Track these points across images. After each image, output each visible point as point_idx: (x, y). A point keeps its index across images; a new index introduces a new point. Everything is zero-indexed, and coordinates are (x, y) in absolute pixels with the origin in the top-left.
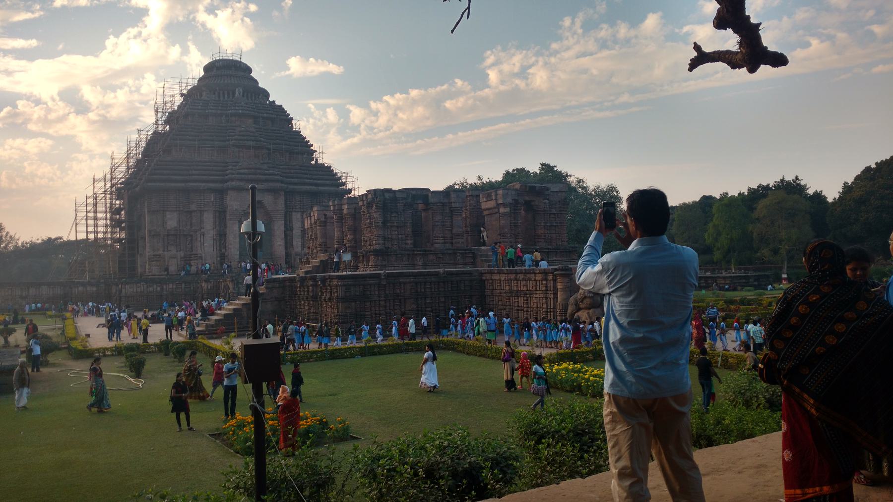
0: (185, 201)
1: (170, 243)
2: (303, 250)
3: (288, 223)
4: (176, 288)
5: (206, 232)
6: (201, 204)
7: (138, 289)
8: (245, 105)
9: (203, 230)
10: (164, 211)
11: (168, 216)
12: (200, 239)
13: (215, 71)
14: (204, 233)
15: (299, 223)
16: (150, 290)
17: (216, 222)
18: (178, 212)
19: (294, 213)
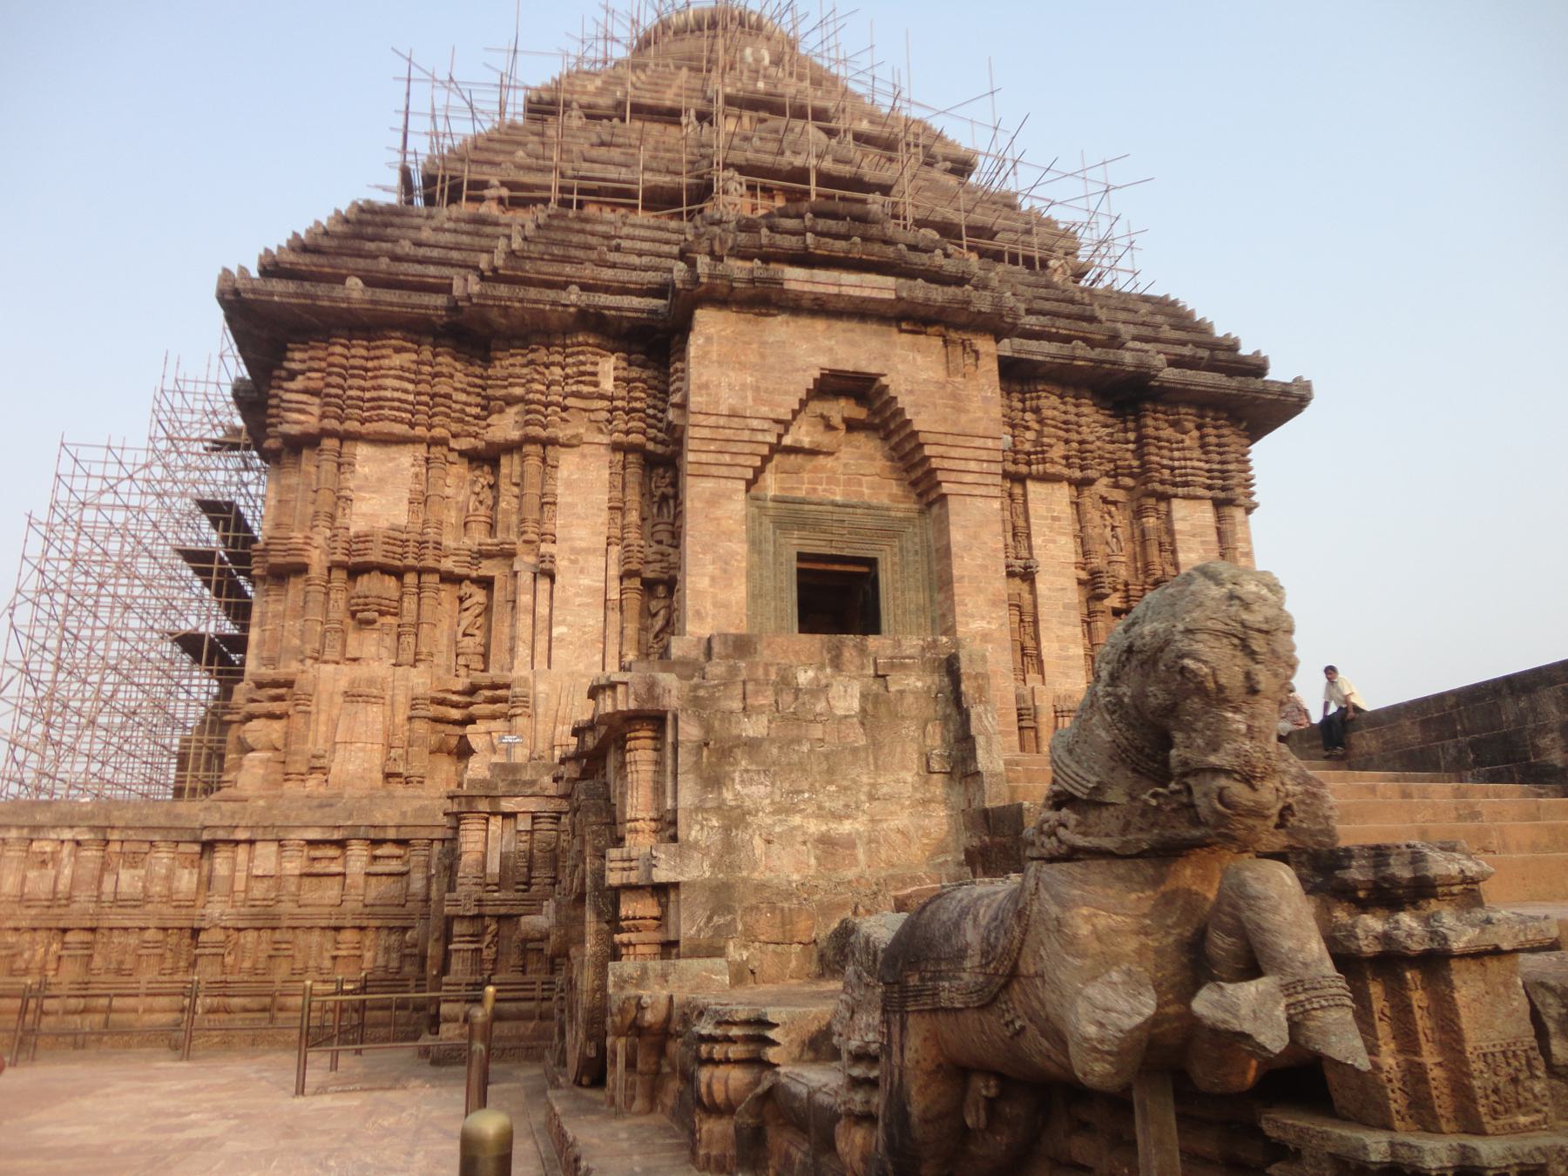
0: (463, 397)
5: (561, 564)
6: (547, 405)
7: (32, 874)
16: (124, 887)
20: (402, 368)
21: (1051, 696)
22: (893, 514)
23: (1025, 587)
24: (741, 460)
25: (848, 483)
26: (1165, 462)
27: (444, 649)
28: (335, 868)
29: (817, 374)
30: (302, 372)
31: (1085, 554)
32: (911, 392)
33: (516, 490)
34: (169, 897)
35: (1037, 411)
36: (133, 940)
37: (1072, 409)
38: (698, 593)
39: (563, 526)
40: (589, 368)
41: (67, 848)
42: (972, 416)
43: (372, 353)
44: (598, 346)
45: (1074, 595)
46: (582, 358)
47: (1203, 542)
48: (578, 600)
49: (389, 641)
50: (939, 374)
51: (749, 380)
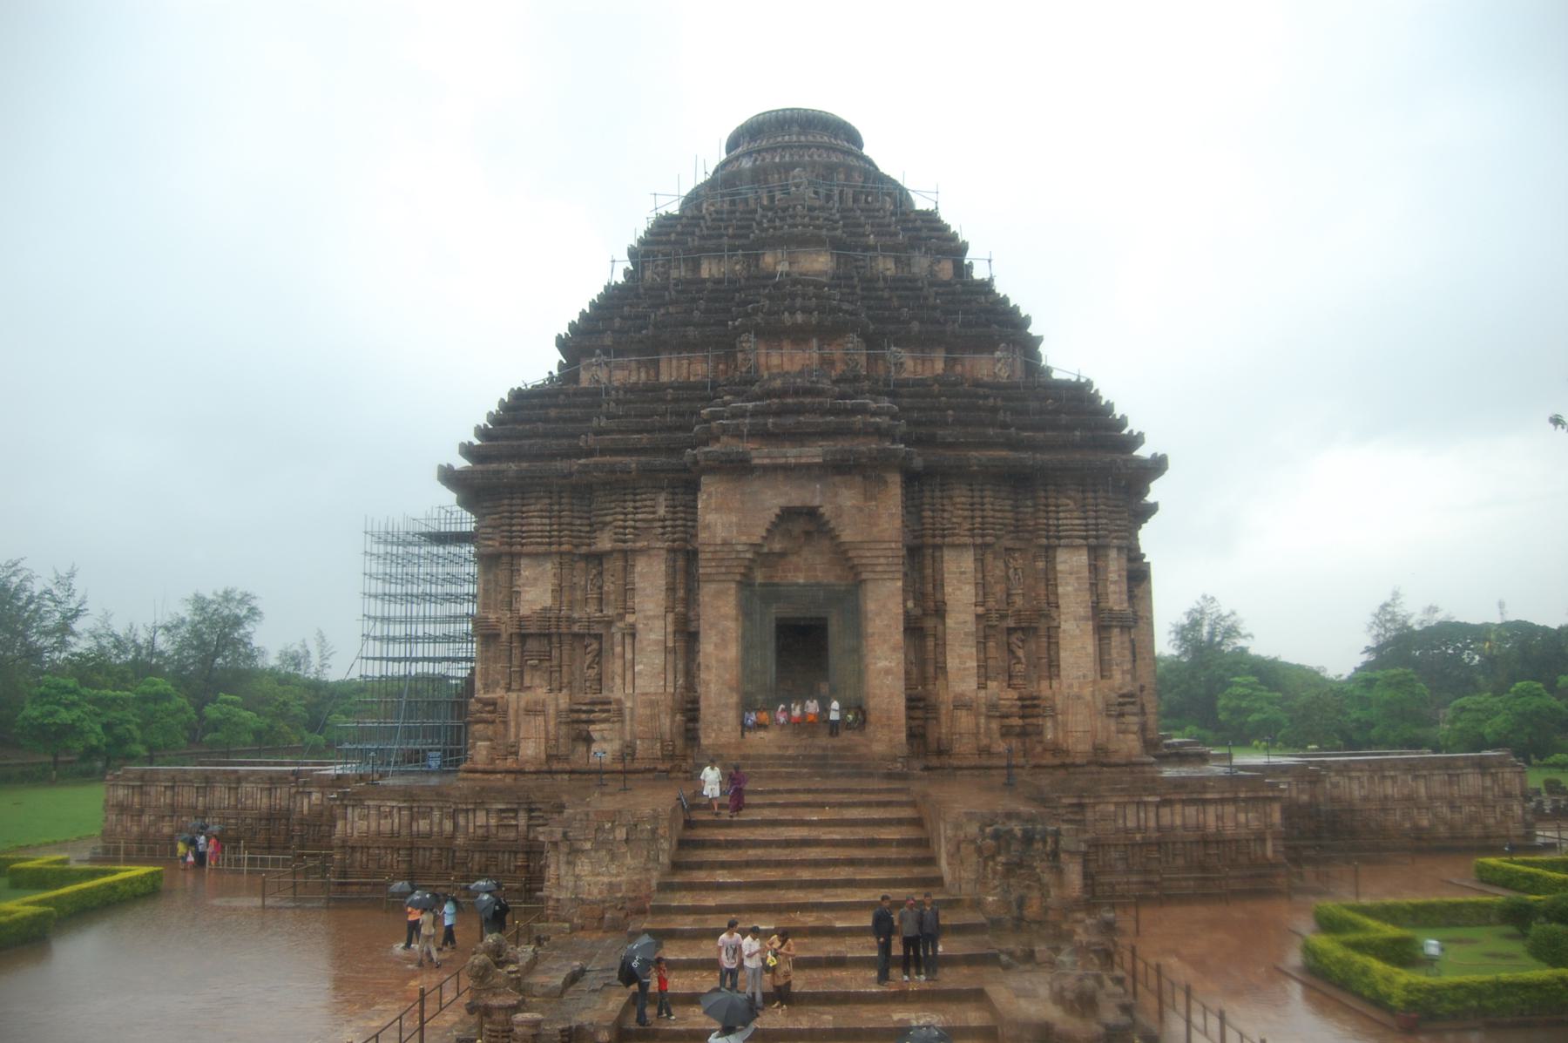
0: (578, 522)
1: (529, 662)
2: (983, 686)
3: (930, 588)
5: (640, 626)
6: (625, 528)
7: (382, 822)
8: (805, 212)
9: (630, 619)
10: (513, 555)
11: (525, 573)
13: (746, 145)
14: (633, 626)
16: (421, 829)
18: (557, 560)
19: (948, 555)
20: (542, 511)
21: (952, 695)
22: (837, 588)
24: (733, 570)
26: (1051, 522)
27: (577, 677)
28: (513, 822)
29: (777, 511)
30: (489, 514)
31: (985, 595)
33: (613, 579)
34: (441, 832)
35: (951, 498)
36: (428, 853)
37: (977, 494)
39: (639, 603)
40: (648, 503)
41: (395, 810)
43: (525, 502)
44: (654, 487)
45: (971, 627)
46: (644, 496)
47: (1078, 578)
48: (649, 649)
49: (546, 676)
51: (734, 519)
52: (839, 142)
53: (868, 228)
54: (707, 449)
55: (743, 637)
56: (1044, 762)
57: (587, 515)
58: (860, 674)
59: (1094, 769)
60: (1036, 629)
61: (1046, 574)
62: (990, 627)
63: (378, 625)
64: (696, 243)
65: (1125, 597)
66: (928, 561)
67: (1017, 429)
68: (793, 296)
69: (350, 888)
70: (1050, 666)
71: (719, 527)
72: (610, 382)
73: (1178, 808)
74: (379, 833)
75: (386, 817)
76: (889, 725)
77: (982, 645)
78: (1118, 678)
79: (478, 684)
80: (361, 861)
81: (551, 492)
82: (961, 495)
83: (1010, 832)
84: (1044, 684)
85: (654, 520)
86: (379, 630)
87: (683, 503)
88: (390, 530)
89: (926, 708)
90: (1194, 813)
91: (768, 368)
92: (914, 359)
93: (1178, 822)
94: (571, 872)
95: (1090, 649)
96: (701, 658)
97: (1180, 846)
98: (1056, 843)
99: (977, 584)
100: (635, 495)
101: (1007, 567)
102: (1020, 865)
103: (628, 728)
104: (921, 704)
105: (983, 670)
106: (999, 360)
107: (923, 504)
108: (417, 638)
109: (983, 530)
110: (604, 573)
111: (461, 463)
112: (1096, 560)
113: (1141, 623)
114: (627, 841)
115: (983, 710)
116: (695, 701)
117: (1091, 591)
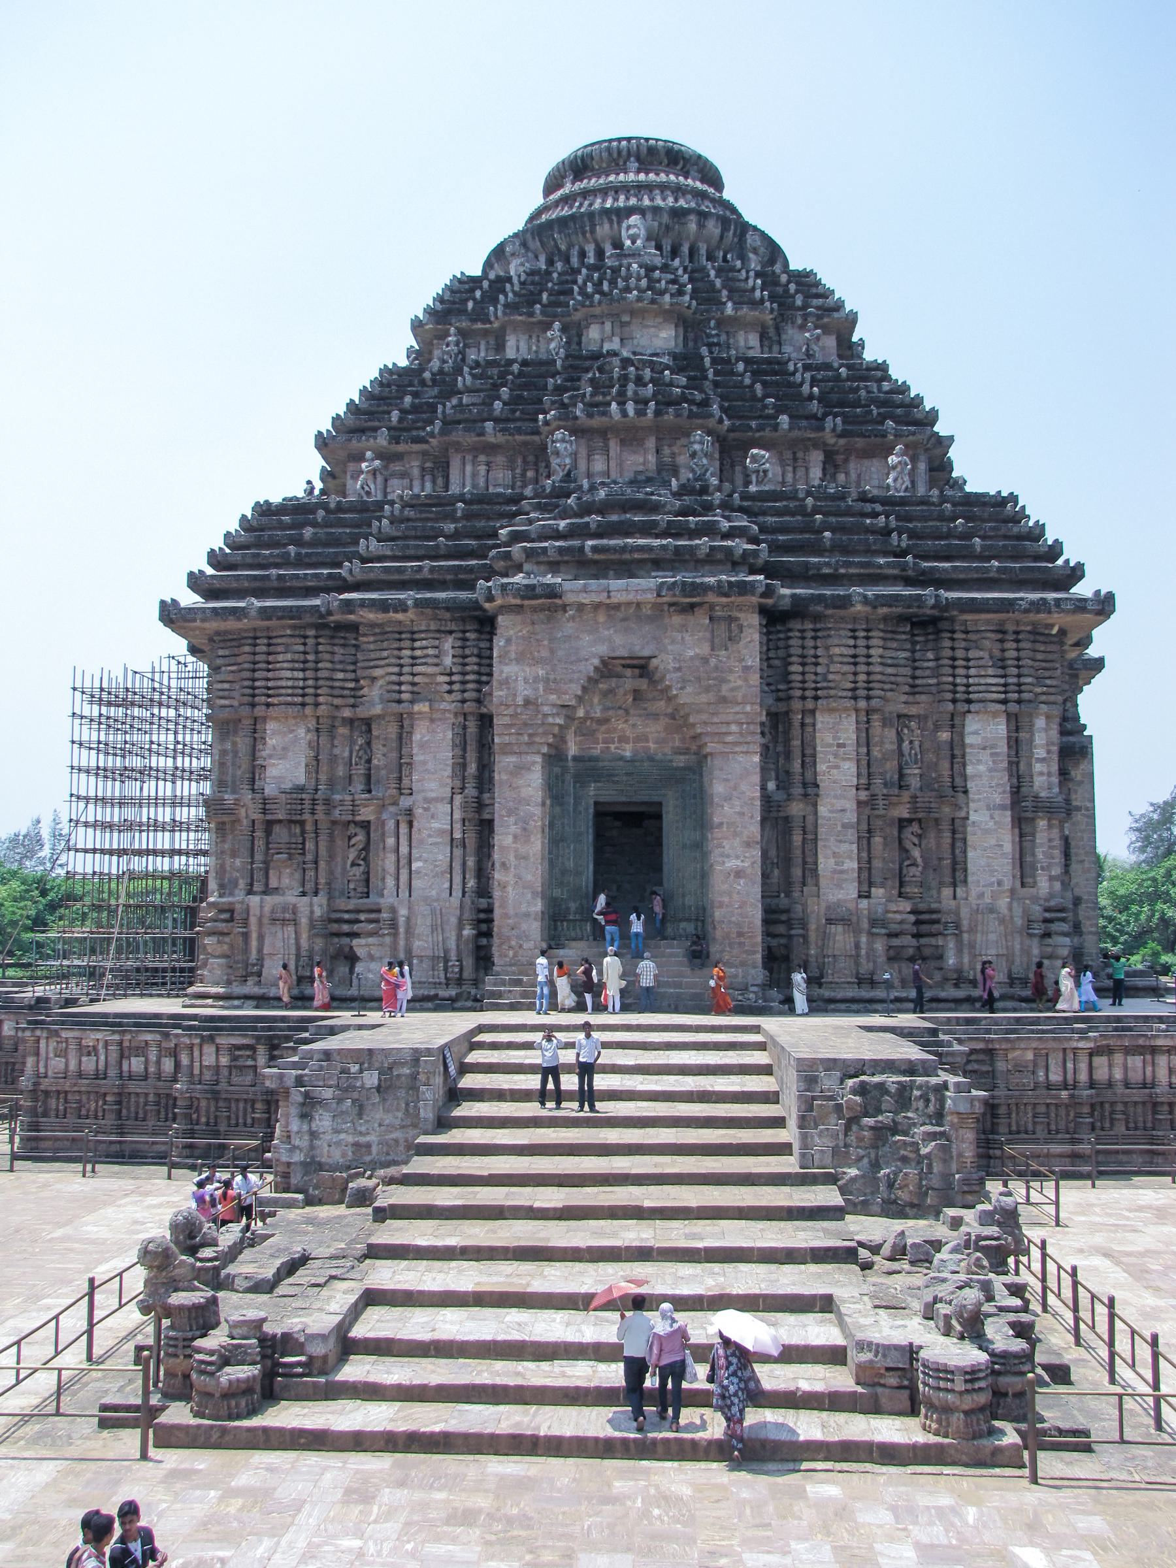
0: (340, 675)
2: (864, 895)
3: (797, 765)
4: (230, 1067)
5: (418, 811)
6: (400, 684)
7: (84, 1059)
8: (643, 271)
9: (405, 802)
11: (271, 742)
12: (391, 841)
15: (850, 767)
16: (134, 1068)
17: (464, 766)
18: (312, 724)
19: (822, 720)
20: (292, 661)
21: (823, 905)
23: (810, 808)
24: (537, 739)
25: (637, 739)
26: (958, 680)
28: (250, 1063)
29: (596, 662)
31: (869, 774)
32: (679, 669)
35: (827, 648)
37: (861, 642)
38: (502, 848)
40: (430, 652)
42: (732, 685)
43: (272, 649)
44: (439, 631)
45: (851, 817)
48: (431, 840)
49: (298, 876)
50: (705, 649)
51: (541, 672)
52: (690, 181)
53: (725, 293)
54: (505, 580)
55: (551, 825)
56: (943, 995)
57: (352, 667)
58: (704, 876)
59: (1010, 1004)
60: (937, 821)
61: (952, 749)
62: (878, 816)
63: (91, 807)
64: (500, 313)
65: (1055, 780)
66: (796, 731)
67: (915, 557)
68: (624, 379)
69: (43, 1145)
70: (954, 870)
71: (521, 683)
72: (385, 494)
73: (1118, 1058)
74: (80, 1075)
75: (89, 1054)
76: (741, 944)
77: (865, 842)
78: (1043, 885)
79: (212, 885)
80: (57, 1110)
81: (305, 637)
82: (839, 646)
83: (881, 1086)
84: (947, 892)
85: (434, 675)
86: (92, 813)
87: (476, 651)
88: (105, 685)
89: (789, 923)
90: (1140, 1065)
91: (589, 475)
92: (783, 465)
93: (1118, 1075)
94: (305, 1127)
95: (1008, 847)
96: (496, 856)
97: (1120, 1107)
98: (942, 1101)
99: (858, 761)
100: (414, 640)
101: (900, 740)
102: (895, 1129)
103: (402, 943)
104: (784, 917)
105: (865, 874)
106: (894, 468)
107: (790, 656)
108: (141, 824)
109: (869, 689)
110: (374, 742)
111: (189, 599)
112: (1017, 730)
113: (1078, 817)
114: (379, 1089)
115: (865, 925)
116: (490, 910)
117: (1010, 770)
